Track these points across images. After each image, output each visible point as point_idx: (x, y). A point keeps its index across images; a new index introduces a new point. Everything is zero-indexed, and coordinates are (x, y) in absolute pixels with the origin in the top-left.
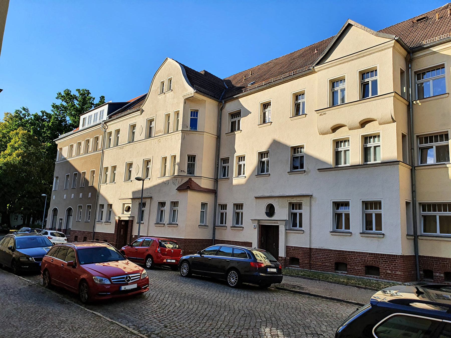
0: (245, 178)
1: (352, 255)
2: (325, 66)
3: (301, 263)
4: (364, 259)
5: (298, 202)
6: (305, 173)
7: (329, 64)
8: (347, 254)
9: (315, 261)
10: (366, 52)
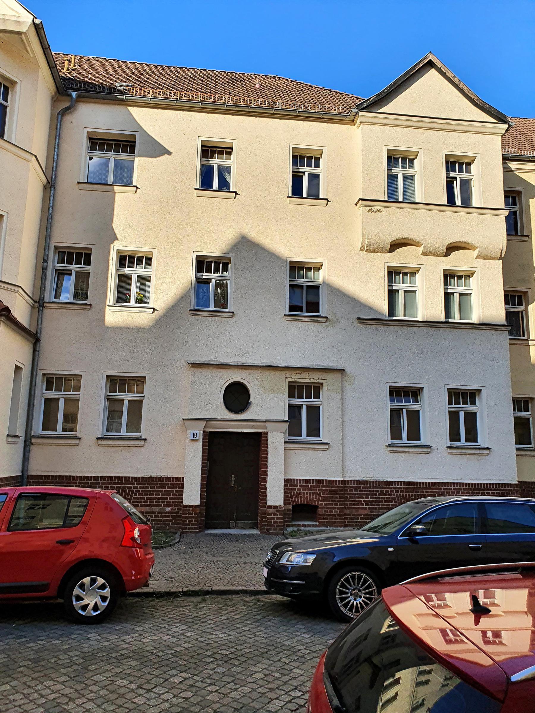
0: (153, 312)
1: (434, 489)
2: (395, 119)
3: (324, 515)
4: (291, 493)
5: (312, 381)
6: (327, 323)
7: (390, 119)
8: (424, 488)
9: (354, 508)
10: (468, 126)
